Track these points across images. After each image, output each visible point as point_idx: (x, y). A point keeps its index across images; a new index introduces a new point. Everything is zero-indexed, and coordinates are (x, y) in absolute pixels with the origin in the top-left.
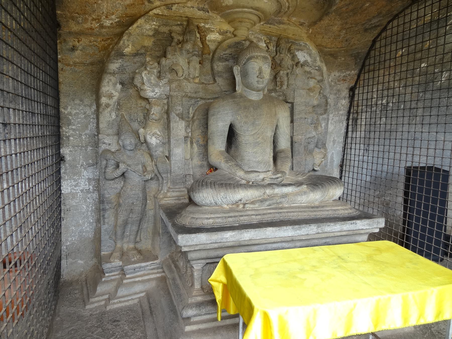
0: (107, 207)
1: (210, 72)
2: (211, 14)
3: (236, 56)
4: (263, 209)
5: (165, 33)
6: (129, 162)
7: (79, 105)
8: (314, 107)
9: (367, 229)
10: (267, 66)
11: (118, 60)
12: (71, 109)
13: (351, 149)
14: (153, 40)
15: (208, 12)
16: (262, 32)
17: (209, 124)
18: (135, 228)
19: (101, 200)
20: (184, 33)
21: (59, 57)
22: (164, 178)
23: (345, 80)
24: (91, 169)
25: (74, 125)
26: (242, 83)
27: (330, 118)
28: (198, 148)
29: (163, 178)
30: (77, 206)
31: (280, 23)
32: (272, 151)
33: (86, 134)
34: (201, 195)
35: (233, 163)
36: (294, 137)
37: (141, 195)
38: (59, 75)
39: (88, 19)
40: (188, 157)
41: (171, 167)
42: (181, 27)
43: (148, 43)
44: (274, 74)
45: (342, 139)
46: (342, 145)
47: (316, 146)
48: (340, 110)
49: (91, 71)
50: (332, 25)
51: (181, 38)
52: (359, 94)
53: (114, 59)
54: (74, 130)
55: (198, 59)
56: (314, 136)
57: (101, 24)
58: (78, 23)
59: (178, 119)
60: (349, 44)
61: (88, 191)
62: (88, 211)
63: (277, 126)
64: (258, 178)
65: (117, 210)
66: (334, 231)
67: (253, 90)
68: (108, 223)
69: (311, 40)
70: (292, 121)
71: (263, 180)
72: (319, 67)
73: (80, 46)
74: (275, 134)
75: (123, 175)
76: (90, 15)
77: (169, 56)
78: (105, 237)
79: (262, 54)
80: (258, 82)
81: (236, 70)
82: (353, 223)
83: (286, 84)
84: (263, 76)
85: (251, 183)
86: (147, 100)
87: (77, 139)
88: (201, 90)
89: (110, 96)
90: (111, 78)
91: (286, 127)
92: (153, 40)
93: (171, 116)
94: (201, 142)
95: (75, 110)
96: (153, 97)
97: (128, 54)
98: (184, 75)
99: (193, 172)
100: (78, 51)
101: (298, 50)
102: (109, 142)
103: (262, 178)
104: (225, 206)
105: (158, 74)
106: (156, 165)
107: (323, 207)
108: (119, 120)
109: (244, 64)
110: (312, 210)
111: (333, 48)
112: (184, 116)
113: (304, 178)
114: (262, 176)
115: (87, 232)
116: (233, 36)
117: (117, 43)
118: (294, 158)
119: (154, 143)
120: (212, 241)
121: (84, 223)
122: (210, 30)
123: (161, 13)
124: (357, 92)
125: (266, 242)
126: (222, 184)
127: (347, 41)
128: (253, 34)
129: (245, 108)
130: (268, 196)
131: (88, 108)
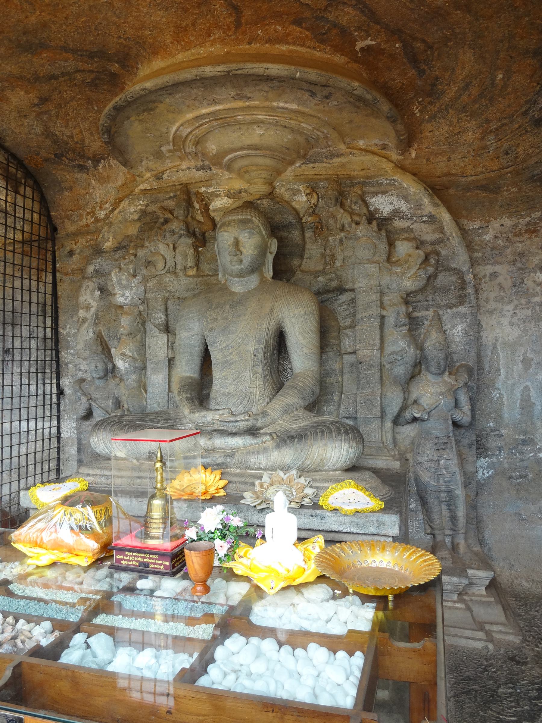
2: (214, 171)
15: (210, 169)
16: (299, 178)
21: (58, 265)
23: (534, 231)
25: (72, 349)
31: (333, 156)
42: (175, 199)
43: (133, 230)
48: (535, 295)
50: (459, 133)
54: (72, 355)
58: (74, 222)
60: (516, 158)
64: (204, 420)
72: (430, 216)
73: (77, 248)
76: (84, 210)
77: (147, 244)
89: (88, 308)
91: (301, 333)
92: (138, 225)
97: (108, 249)
98: (167, 267)
100: (76, 256)
101: (376, 194)
111: (482, 173)
113: (302, 425)
123: (149, 188)
128: (282, 185)
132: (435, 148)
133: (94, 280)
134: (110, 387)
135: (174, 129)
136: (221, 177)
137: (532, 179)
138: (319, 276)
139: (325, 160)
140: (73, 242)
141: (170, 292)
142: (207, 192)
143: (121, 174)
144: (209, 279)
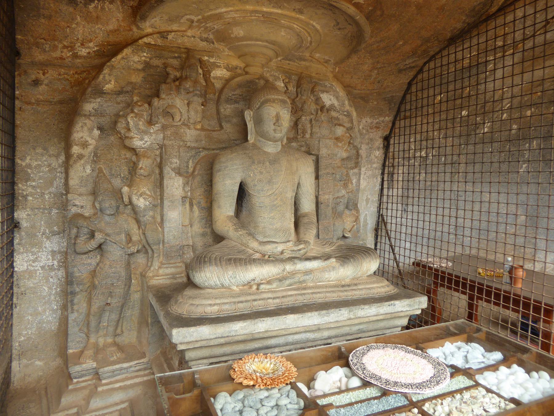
0: (77, 290)
1: (215, 117)
2: (216, 45)
3: (248, 97)
4: (282, 290)
5: (159, 67)
6: (109, 230)
7: (42, 155)
8: (343, 160)
9: (407, 311)
10: (286, 112)
11: (95, 99)
12: (31, 159)
13: (387, 209)
14: (142, 75)
15: (213, 43)
17: (213, 182)
18: (114, 316)
19: (69, 280)
20: (182, 68)
21: (17, 92)
22: (155, 251)
24: (56, 239)
25: (34, 181)
26: (256, 131)
27: (362, 173)
28: (199, 211)
29: (153, 251)
30: (35, 288)
31: (301, 59)
32: (293, 215)
33: (50, 193)
34: (203, 274)
35: (245, 232)
36: (320, 196)
37: (123, 274)
38: (17, 116)
39: (57, 46)
40: (187, 222)
41: (164, 236)
42: (179, 60)
43: (137, 78)
44: (294, 119)
45: (376, 198)
46: (377, 205)
47: (347, 207)
48: (374, 163)
49: (60, 111)
51: (178, 74)
52: (394, 144)
53: (91, 97)
54: (33, 187)
55: (200, 100)
56: (344, 196)
57: (74, 53)
58: (45, 51)
59: (174, 174)
60: (382, 86)
61: (51, 268)
62: (50, 295)
63: (299, 184)
64: (275, 251)
65: (90, 293)
66: (368, 315)
67: (270, 140)
68: (78, 311)
69: (338, 80)
70: (317, 177)
71: (282, 253)
72: (348, 111)
73: (45, 80)
74: (296, 194)
75: (100, 247)
77: (163, 96)
78: (73, 329)
79: (280, 97)
80: (275, 130)
81: (248, 115)
82: (391, 305)
83: (309, 132)
84: (282, 123)
85: (267, 257)
86: (133, 150)
87: (38, 198)
88: (203, 139)
89: (85, 145)
90: (86, 121)
92: (142, 75)
93: (165, 172)
94: (203, 204)
95: (36, 161)
96: (141, 146)
97: (109, 91)
98: (183, 119)
99: (193, 242)
100: (43, 86)
101: (323, 92)
102: (81, 203)
103: (281, 250)
104: (235, 288)
105: (149, 118)
106: (144, 234)
107: (356, 285)
108: (95, 174)
109: (258, 108)
110: (342, 289)
111: (364, 89)
112: (182, 171)
113: (332, 248)
114: (280, 248)
115: (49, 322)
116: (244, 73)
117: (96, 77)
118: (320, 222)
119: (142, 206)
120: (217, 335)
121: (45, 311)
122: (215, 66)
123: (153, 43)
124: (392, 142)
125: (286, 333)
126: (230, 260)
127: (379, 82)
129: (259, 162)
130: (289, 273)
131: (54, 158)
132: (347, 69)
133: (92, 118)
134: (120, 222)
135: (224, 10)
136: (222, 52)
137: (385, 99)
138: (292, 142)
139: (296, 61)
140: (41, 72)
141: (184, 141)
142: (209, 61)
143: (114, 20)
144: (211, 134)
